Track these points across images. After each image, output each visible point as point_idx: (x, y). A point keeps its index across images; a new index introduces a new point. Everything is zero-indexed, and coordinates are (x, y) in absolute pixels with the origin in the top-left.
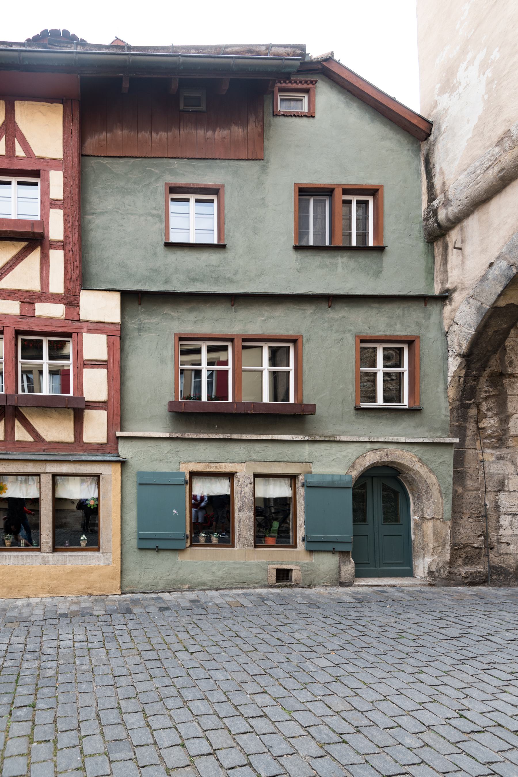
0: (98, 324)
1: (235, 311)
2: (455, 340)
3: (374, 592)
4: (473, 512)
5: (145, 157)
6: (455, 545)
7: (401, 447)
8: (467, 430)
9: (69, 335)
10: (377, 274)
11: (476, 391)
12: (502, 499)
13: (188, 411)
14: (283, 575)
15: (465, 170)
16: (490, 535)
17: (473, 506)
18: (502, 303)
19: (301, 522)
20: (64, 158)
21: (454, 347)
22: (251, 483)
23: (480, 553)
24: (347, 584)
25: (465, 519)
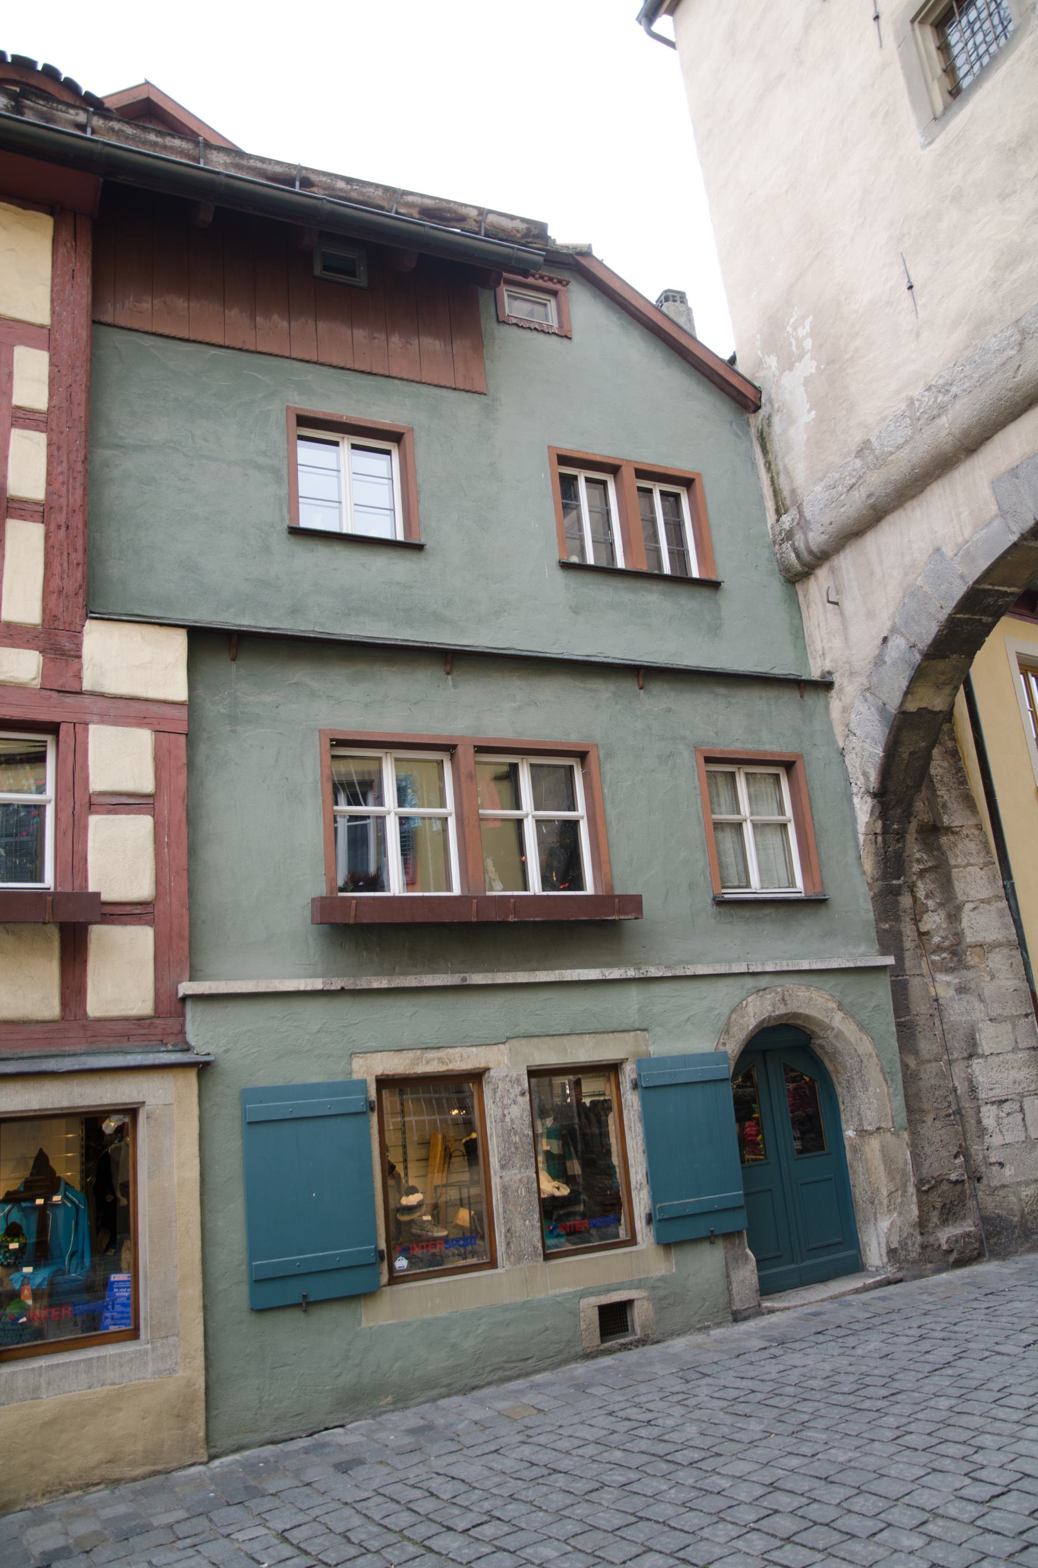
3: (800, 1318)
4: (940, 1106)
6: (921, 1182)
7: (805, 979)
8: (904, 939)
11: (904, 861)
12: (977, 1073)
13: (365, 921)
14: (614, 1319)
16: (972, 1151)
17: (937, 1093)
19: (640, 1177)
21: (857, 778)
22: (523, 1094)
23: (963, 1192)
24: (745, 1314)
25: (929, 1123)
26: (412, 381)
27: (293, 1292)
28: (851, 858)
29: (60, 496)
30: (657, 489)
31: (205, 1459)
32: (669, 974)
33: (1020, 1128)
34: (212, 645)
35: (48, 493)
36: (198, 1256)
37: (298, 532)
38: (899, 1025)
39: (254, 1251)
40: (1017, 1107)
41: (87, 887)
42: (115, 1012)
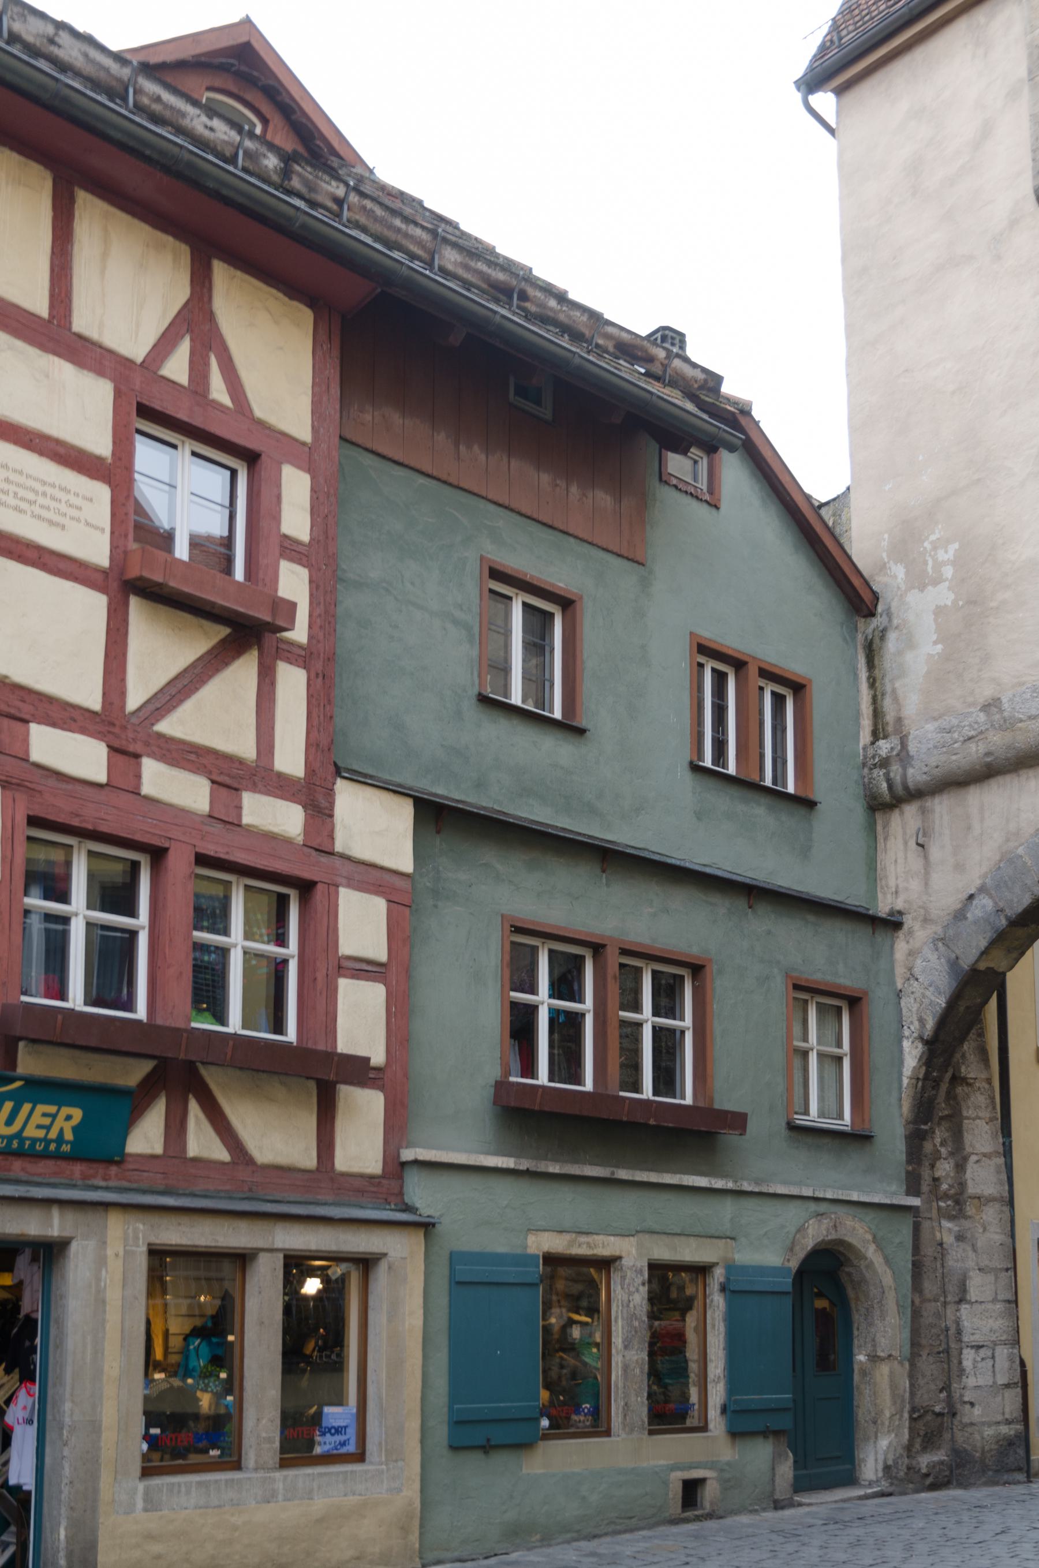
0: (370, 869)
1: (608, 885)
5: (445, 482)
6: (913, 1410)
7: (852, 1210)
10: (805, 852)
17: (933, 1331)
23: (942, 1423)
25: (924, 1357)
29: (319, 641)
32: (757, 1190)
33: (990, 1373)
34: (434, 816)
40: (989, 1354)
41: (336, 1048)
42: (356, 1168)
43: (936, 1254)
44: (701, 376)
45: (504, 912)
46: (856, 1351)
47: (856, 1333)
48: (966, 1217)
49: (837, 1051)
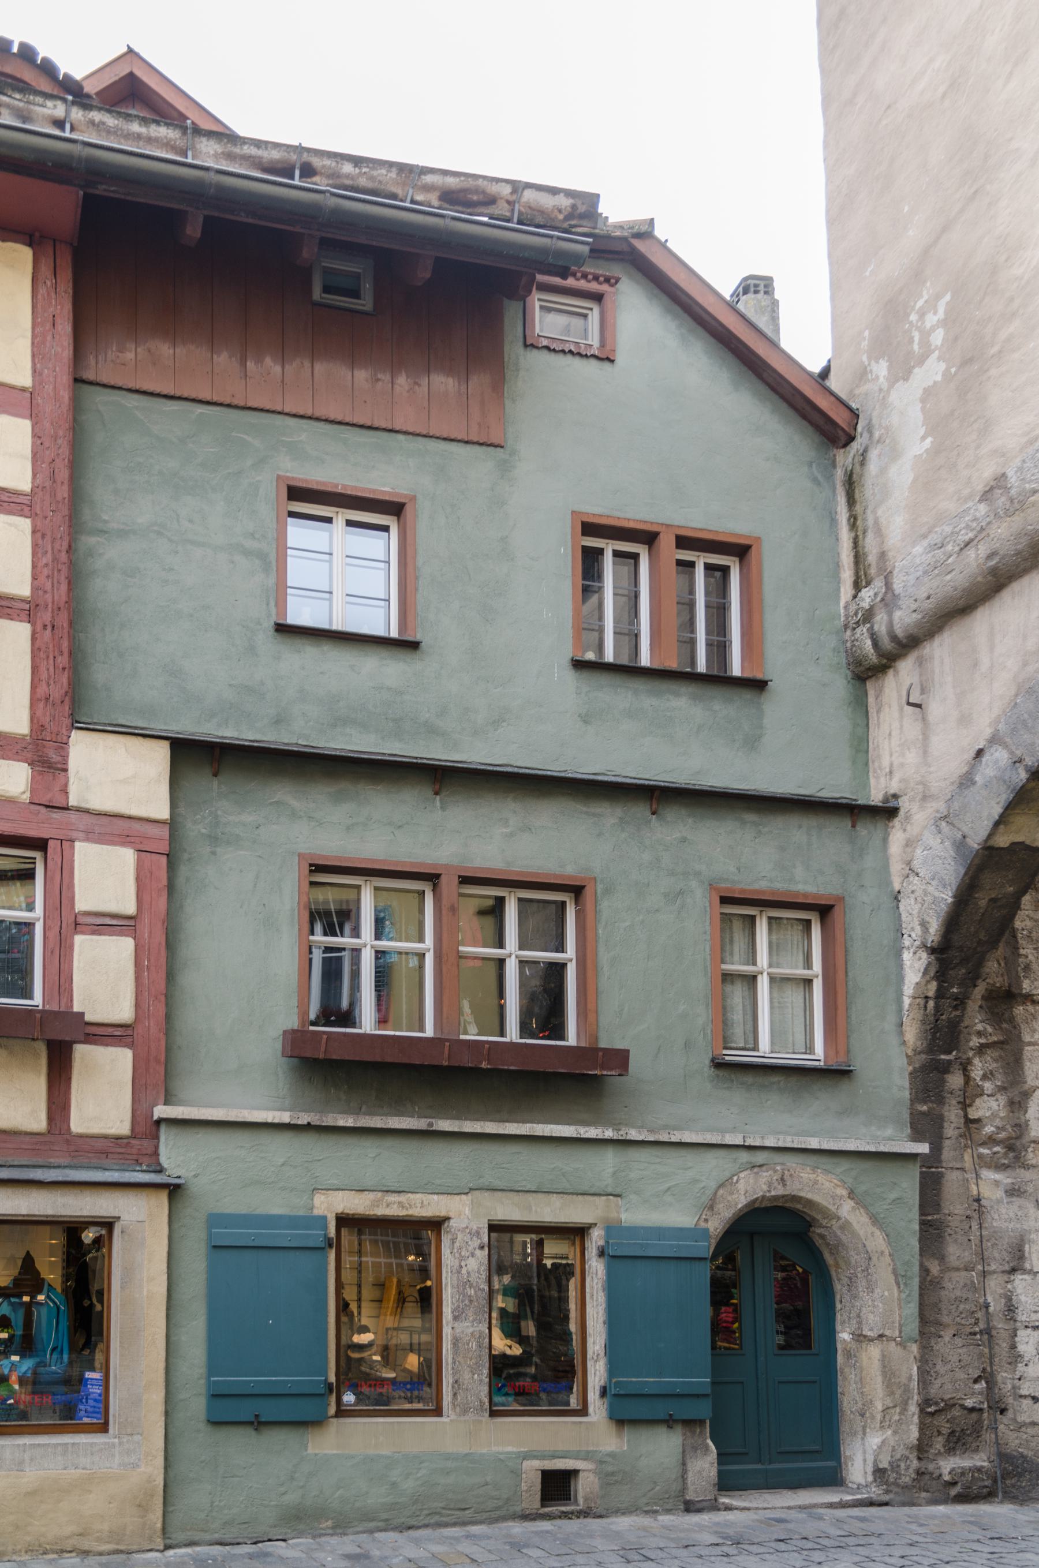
2: (915, 912)
3: (761, 1522)
4: (963, 1322)
6: (926, 1402)
7: (812, 1160)
8: (946, 1125)
9: (40, 845)
10: (752, 743)
11: (960, 1032)
12: (1019, 1291)
13: (334, 1057)
14: (557, 1486)
15: (924, 537)
16: (999, 1378)
17: (962, 1306)
18: (1003, 841)
19: (597, 1347)
20: (34, 386)
21: (913, 929)
22: (482, 1248)
23: (979, 1421)
24: (699, 1506)
25: (947, 1339)
26: (418, 435)
27: (246, 1410)
28: (890, 1025)
29: (45, 592)
30: (701, 560)
31: (161, 1547)
32: (652, 1139)
34: (196, 757)
35: (34, 589)
36: (162, 1365)
37: (283, 629)
38: (923, 1223)
39: (213, 1367)
41: (72, 1007)
42: (95, 1129)
43: (969, 1212)
44: (565, 202)
45: (302, 851)
46: (838, 1327)
47: (838, 1306)
48: (1026, 1167)
49: (806, 973)
